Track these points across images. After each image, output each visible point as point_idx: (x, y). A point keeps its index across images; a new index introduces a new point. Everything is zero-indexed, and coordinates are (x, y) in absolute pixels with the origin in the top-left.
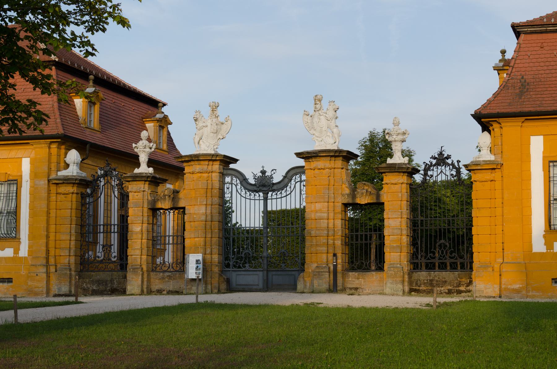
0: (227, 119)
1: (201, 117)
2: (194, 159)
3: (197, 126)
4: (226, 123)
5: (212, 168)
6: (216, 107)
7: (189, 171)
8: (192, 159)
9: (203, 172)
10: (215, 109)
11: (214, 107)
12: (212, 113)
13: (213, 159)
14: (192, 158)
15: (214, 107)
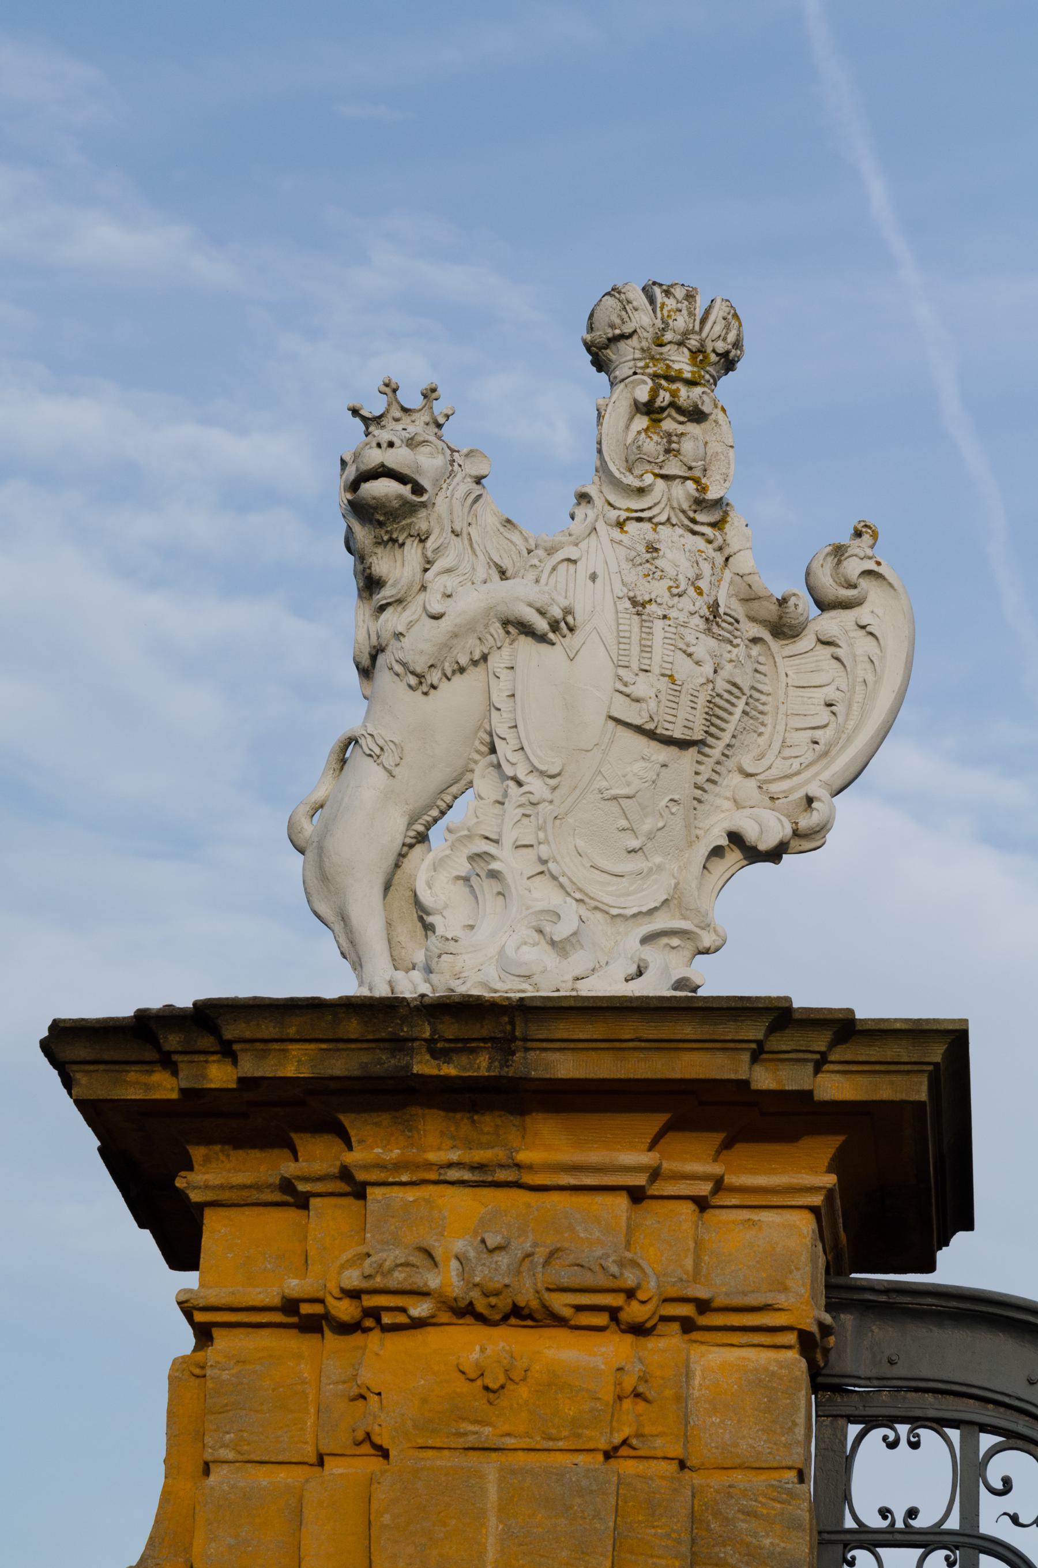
0: (853, 567)
1: (462, 486)
2: (424, 1066)
3: (392, 621)
4: (832, 623)
5: (699, 1244)
6: (698, 354)
7: (294, 1286)
8: (387, 1062)
9: (560, 1303)
10: (686, 395)
11: (681, 362)
12: (652, 446)
13: (764, 1079)
14: (399, 1044)
15: (681, 362)
